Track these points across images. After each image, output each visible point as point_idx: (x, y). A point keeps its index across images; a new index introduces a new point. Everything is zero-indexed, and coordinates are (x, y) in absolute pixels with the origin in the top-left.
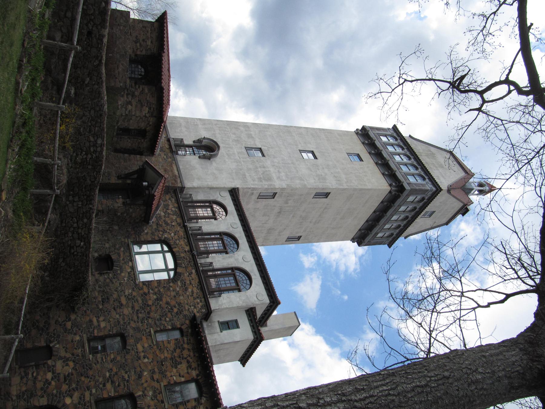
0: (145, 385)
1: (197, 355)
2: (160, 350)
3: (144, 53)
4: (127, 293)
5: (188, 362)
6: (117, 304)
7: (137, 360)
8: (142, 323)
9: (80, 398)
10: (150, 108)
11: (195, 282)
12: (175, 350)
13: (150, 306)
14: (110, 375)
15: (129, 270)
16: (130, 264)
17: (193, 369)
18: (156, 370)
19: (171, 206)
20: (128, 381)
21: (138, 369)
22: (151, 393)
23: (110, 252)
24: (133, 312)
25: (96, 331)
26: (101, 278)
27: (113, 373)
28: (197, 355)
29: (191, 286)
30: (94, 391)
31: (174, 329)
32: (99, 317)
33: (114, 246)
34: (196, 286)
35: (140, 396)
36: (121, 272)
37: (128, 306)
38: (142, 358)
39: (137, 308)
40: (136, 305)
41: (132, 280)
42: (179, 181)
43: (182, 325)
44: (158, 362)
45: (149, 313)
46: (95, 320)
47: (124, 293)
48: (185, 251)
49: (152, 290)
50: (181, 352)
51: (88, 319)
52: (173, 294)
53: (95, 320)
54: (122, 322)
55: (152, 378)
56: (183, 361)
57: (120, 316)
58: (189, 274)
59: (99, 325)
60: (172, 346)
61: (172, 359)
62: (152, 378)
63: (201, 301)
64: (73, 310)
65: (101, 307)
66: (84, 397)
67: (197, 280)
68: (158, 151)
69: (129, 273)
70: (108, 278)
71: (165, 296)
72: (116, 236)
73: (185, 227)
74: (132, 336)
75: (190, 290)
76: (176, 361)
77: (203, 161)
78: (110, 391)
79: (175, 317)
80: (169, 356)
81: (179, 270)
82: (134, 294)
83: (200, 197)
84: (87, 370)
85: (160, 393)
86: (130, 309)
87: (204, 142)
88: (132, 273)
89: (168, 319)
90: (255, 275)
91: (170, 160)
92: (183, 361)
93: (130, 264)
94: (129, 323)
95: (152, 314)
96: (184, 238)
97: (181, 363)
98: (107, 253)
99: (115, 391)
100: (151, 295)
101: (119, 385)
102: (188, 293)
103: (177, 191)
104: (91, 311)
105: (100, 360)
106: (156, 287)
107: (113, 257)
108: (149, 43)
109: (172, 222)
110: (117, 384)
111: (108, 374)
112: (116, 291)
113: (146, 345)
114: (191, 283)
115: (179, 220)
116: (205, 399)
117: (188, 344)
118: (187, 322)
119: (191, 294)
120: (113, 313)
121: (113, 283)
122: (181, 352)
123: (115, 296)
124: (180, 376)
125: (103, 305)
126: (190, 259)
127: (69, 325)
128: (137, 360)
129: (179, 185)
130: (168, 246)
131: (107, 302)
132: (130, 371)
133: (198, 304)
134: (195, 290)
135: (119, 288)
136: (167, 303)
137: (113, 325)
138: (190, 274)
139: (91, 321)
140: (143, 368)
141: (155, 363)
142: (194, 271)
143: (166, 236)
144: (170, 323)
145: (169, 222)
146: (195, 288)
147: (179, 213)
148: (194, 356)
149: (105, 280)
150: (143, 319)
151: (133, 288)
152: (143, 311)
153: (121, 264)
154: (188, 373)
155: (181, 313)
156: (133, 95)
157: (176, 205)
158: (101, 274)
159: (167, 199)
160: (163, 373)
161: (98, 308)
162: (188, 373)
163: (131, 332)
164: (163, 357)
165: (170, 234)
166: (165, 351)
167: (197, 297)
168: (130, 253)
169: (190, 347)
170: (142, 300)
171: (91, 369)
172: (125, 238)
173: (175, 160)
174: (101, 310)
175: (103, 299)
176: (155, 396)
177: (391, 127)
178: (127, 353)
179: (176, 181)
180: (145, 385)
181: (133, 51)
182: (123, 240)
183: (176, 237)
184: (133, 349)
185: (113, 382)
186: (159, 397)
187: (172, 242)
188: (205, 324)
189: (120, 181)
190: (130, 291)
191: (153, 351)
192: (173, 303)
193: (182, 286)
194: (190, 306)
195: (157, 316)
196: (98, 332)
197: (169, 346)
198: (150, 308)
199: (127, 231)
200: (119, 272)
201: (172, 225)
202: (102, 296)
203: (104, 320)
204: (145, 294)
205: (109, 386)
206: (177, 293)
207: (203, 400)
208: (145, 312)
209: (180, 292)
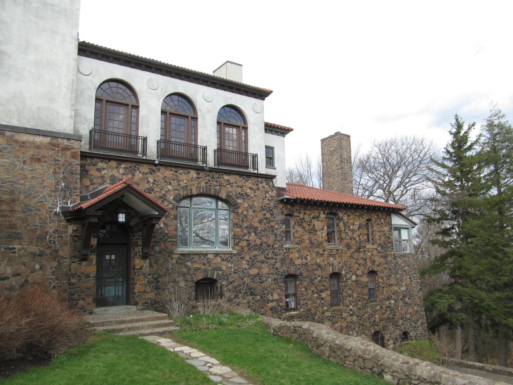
1: (309, 207)
2: (302, 242)
4: (247, 267)
5: (314, 218)
6: (257, 279)
7: (308, 266)
8: (277, 255)
9: (329, 320)
12: (304, 228)
13: (262, 242)
14: (317, 293)
15: (219, 259)
16: (209, 256)
17: (319, 215)
18: (316, 250)
19: (115, 173)
20: (322, 278)
21: (315, 267)
22: (332, 259)
23: (193, 281)
24: (267, 263)
25: (281, 304)
26: (227, 294)
27: (315, 290)
28: (309, 207)
29: (244, 188)
30: (325, 308)
31: (286, 222)
32: (269, 300)
33: (184, 274)
34: (244, 181)
35: (332, 269)
36: (221, 269)
37: (261, 267)
38: (306, 261)
39: (263, 258)
41: (232, 258)
42: (65, 142)
43: (283, 213)
44: (311, 247)
45: (268, 246)
46: (271, 305)
47: (246, 269)
48: (198, 178)
49: (244, 236)
50: (305, 221)
52: (251, 212)
53: (271, 305)
54: (276, 276)
56: (313, 223)
57: (269, 277)
58: (230, 184)
59: (276, 300)
60: (300, 229)
63: (261, 183)
65: (258, 297)
66: (328, 317)
67: (237, 177)
69: (223, 260)
70: (227, 286)
71: (252, 223)
72: (167, 270)
73: (161, 164)
74: (288, 268)
75: (248, 191)
76: (312, 229)
79: (274, 217)
80: (308, 234)
82: (247, 257)
83: (89, 111)
84: (311, 313)
86: (263, 266)
88: (223, 256)
89: (276, 227)
90: (231, 98)
92: (313, 223)
93: (209, 256)
94: (277, 269)
95: (270, 242)
96: (176, 172)
97: (314, 225)
98: (194, 285)
99: (327, 290)
100: (251, 238)
101: (324, 286)
102: (252, 195)
104: (262, 308)
105: (306, 302)
106: (242, 231)
107: (200, 277)
109: (148, 182)
110: (323, 288)
111: (316, 295)
112: (243, 279)
113: (297, 255)
114: (241, 187)
115: (145, 169)
116: (340, 213)
117: (300, 213)
118: (281, 206)
119: (253, 191)
121: (234, 281)
122: (305, 221)
123: (247, 280)
124: (323, 230)
125: (256, 295)
126: (209, 176)
128: (308, 266)
130: (185, 198)
131: (254, 289)
132: (315, 275)
133: (264, 187)
134: (247, 183)
135: (241, 274)
136: (260, 222)
137: (277, 286)
139: (271, 309)
140: (313, 262)
141: (311, 250)
142: (226, 177)
143: (171, 198)
144: (280, 225)
145: (147, 186)
146: (247, 183)
147: (129, 165)
148: (310, 210)
149: (230, 291)
150: (273, 253)
151: (242, 258)
152: (266, 252)
153: (211, 268)
154: (322, 221)
155: (272, 210)
157: (114, 164)
158: (222, 295)
159: (98, 174)
160: (320, 245)
161: (259, 300)
162: (322, 221)
163: (284, 268)
164: (308, 241)
165: (169, 191)
166: (304, 237)
167: (257, 185)
168: (196, 254)
169: (303, 212)
170: (255, 249)
171: (310, 310)
172: (172, 259)
174: (262, 297)
175: (252, 294)
176: (333, 256)
178: (302, 275)
179: (66, 149)
180: (326, 263)
182: (174, 261)
183: (174, 183)
184: (300, 269)
185: (321, 291)
186: (334, 252)
189: (93, 257)
190: (244, 262)
191: (302, 249)
192: (260, 215)
193: (244, 199)
194: (266, 197)
195: (272, 238)
196: (282, 302)
197: (299, 233)
198: (264, 243)
199: (160, 252)
200: (220, 272)
201: (154, 183)
202: (248, 295)
203: (272, 295)
205: (323, 295)
206: (251, 207)
207: (340, 214)
208: (267, 249)
209: (249, 203)
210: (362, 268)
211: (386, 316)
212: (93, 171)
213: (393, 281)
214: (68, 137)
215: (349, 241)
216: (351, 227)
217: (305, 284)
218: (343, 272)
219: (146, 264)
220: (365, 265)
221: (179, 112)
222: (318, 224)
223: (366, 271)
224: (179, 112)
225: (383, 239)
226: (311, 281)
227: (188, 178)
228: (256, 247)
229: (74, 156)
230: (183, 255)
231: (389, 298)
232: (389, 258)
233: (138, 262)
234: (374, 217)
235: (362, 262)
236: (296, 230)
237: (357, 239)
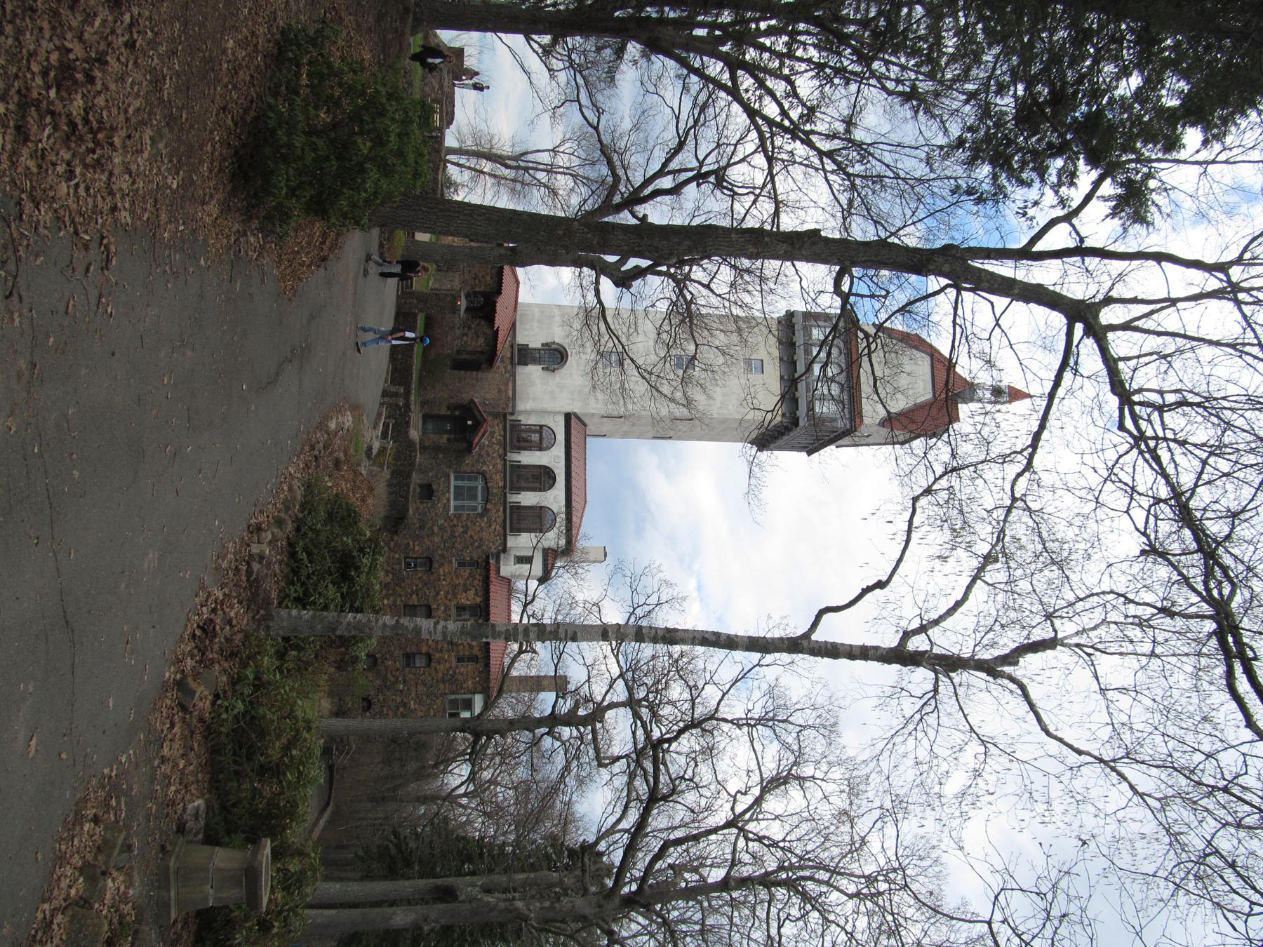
3: (482, 289)
11: (500, 520)
60: (467, 574)
64: (396, 532)
68: (498, 363)
77: (546, 373)
78: (414, 600)
83: (532, 420)
103: (505, 414)
108: (488, 278)
115: (501, 451)
127: (392, 544)
136: (471, 537)
156: (470, 328)
160: (455, 595)
163: (437, 558)
173: (514, 375)
176: (445, 611)
187: (488, 476)
188: (502, 556)
195: (460, 547)
211: (389, 675)
212: (496, 422)
213: (420, 688)
214: (514, 406)
219: (444, 441)
221: (543, 478)
222: (472, 593)
224: (543, 478)
225: (460, 677)
226: (425, 584)
227: (497, 480)
231: (405, 682)
232: (442, 686)
233: (446, 436)
234: (480, 666)
236: (466, 572)
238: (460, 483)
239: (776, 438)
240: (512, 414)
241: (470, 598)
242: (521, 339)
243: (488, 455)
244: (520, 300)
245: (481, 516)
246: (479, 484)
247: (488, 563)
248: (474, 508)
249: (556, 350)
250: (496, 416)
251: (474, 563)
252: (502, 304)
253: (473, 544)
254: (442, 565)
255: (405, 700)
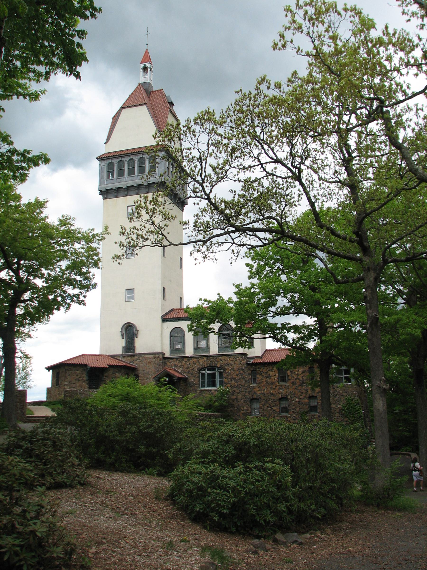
0: (277, 392)
3: (84, 375)
5: (269, 370)
10: (116, 372)
21: (269, 394)
39: (239, 391)
40: (236, 391)
42: (158, 355)
46: (242, 412)
51: (241, 415)
52: (232, 371)
53: (242, 412)
55: (274, 389)
61: (267, 378)
62: (274, 389)
68: (134, 365)
75: (231, 362)
81: (218, 365)
85: (281, 386)
87: (124, 332)
91: (141, 358)
108: (78, 372)
113: (258, 389)
115: (186, 360)
118: (249, 367)
120: (240, 403)
129: (161, 356)
134: (230, 359)
136: (237, 375)
138: (221, 360)
139: (243, 414)
142: (220, 358)
157: (175, 360)
160: (273, 383)
163: (251, 396)
173: (140, 355)
177: (98, 162)
179: (158, 358)
180: (277, 392)
181: (84, 382)
183: (197, 363)
185: (273, 407)
187: (201, 367)
192: (237, 372)
195: (244, 382)
204: (231, 386)
205: (274, 408)
210: (304, 395)
212: (168, 364)
214: (159, 353)
215: (294, 381)
216: (296, 373)
217: (263, 403)
218: (289, 397)
220: (306, 393)
222: (271, 373)
223: (307, 396)
226: (267, 402)
228: (234, 387)
229: (160, 360)
230: (201, 391)
235: (304, 391)
237: (301, 379)
238: (206, 384)
239: (176, 195)
240: (163, 354)
241: (274, 375)
242: (119, 351)
243: (188, 367)
244: (98, 353)
245: (225, 370)
246: (206, 372)
247: (252, 364)
248: (221, 374)
249: (126, 330)
250: (165, 364)
251: (253, 372)
252: (92, 364)
253: (242, 374)
254: (255, 392)
255: (338, 411)
